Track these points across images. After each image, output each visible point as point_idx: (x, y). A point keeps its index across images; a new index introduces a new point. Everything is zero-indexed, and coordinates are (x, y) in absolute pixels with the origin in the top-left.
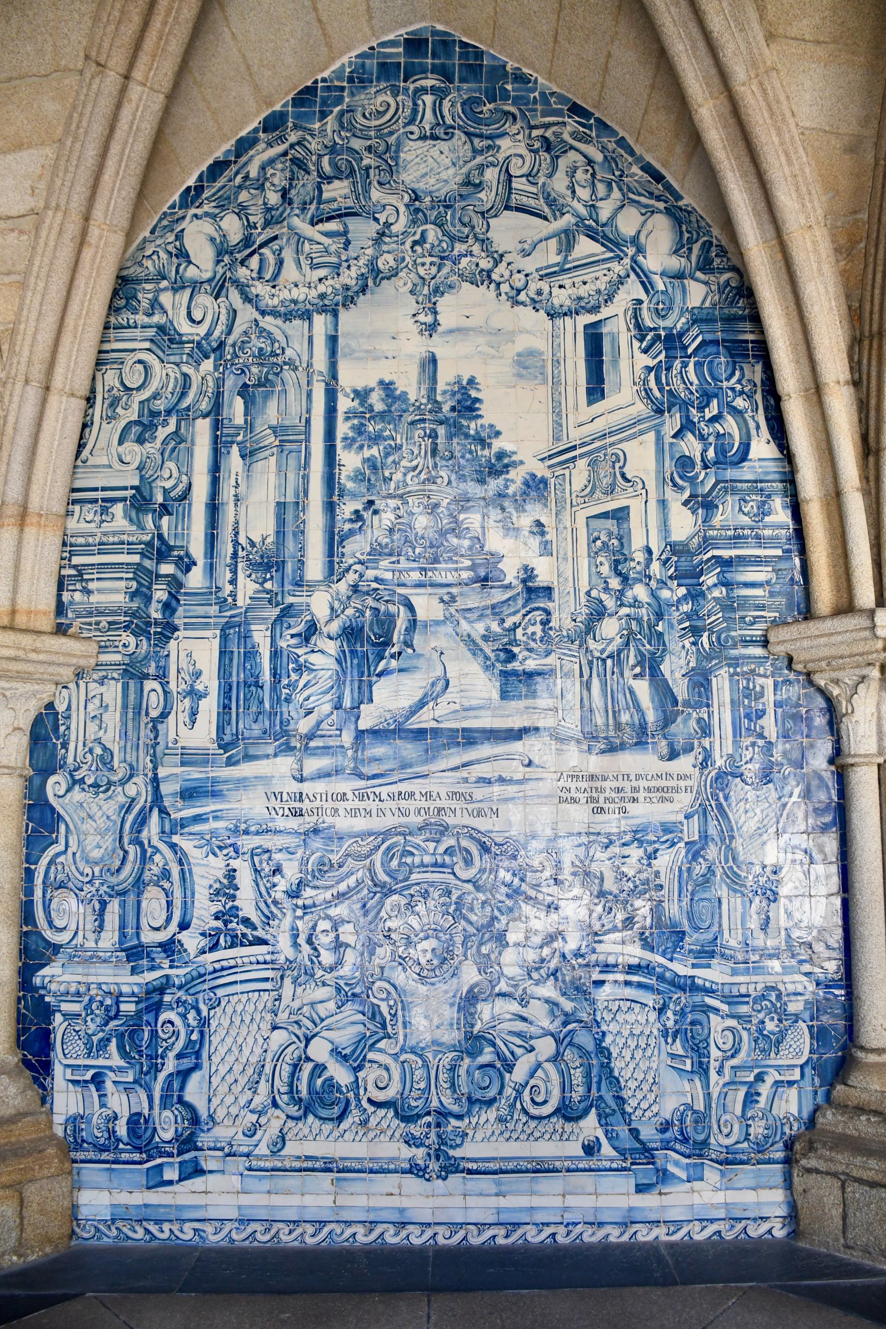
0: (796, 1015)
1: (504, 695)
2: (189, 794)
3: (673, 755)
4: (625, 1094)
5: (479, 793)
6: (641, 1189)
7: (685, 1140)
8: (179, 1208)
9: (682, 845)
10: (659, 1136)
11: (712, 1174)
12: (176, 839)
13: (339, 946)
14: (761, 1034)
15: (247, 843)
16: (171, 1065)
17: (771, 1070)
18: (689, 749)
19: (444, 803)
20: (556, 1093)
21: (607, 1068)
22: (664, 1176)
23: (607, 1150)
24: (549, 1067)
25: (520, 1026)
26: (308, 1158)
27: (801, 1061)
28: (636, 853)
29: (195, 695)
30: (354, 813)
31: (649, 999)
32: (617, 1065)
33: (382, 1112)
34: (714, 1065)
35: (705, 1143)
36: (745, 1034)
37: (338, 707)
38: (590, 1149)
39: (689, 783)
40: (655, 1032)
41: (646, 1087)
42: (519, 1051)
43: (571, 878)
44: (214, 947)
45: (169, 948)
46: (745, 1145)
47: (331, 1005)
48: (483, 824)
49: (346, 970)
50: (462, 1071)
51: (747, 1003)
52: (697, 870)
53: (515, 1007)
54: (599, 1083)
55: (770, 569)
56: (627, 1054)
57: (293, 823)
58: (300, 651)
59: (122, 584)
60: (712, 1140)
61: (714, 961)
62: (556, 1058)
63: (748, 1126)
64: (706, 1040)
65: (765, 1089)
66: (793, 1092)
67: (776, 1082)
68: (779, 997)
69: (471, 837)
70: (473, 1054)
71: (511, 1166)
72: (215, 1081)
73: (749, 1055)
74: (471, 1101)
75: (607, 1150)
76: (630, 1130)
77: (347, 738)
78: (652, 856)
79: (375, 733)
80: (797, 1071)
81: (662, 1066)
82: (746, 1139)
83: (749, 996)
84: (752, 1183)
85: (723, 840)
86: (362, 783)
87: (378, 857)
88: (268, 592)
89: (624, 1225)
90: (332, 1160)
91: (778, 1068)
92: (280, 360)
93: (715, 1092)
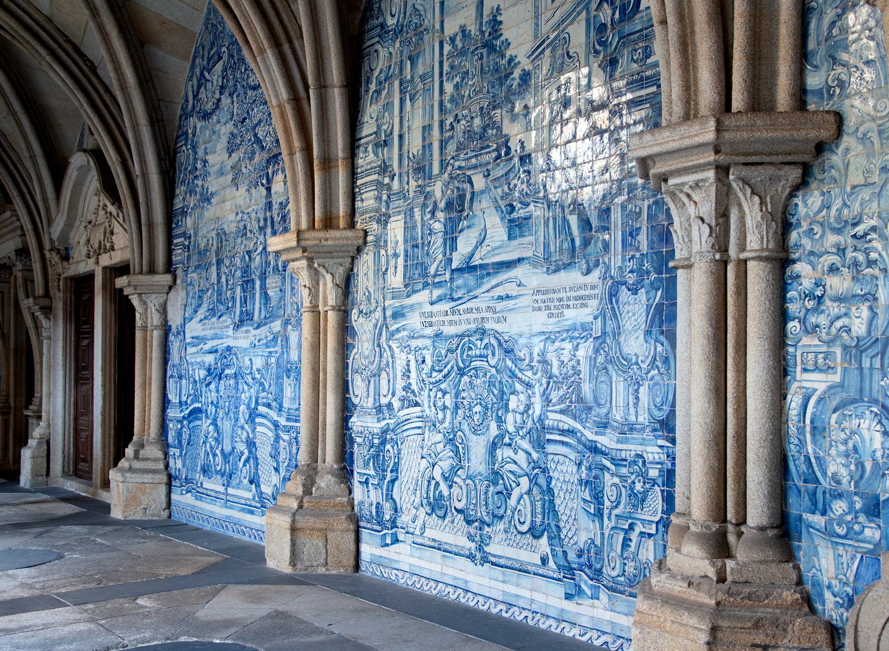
0: (654, 480)
2: (397, 315)
3: (588, 271)
4: (562, 524)
5: (499, 306)
6: (568, 597)
7: (590, 567)
8: (392, 560)
9: (591, 340)
10: (577, 560)
11: (604, 596)
12: (391, 343)
13: (445, 408)
14: (633, 492)
15: (414, 343)
17: (638, 522)
18: (597, 265)
19: (484, 315)
21: (552, 502)
22: (580, 592)
23: (551, 564)
24: (525, 496)
26: (434, 540)
27: (657, 519)
28: (568, 346)
29: (396, 255)
30: (451, 323)
31: (573, 455)
32: (557, 502)
33: (459, 516)
34: (606, 512)
35: (600, 571)
36: (623, 490)
37: (445, 255)
38: (544, 561)
39: (596, 291)
40: (576, 481)
41: (571, 521)
42: (514, 485)
43: (537, 364)
46: (622, 579)
47: (441, 445)
48: (499, 327)
49: (447, 424)
50: (490, 494)
51: (625, 466)
52: (599, 361)
54: (548, 513)
55: (648, 105)
56: (562, 494)
57: (429, 331)
58: (431, 222)
59: (372, 193)
60: (604, 571)
61: (608, 431)
62: (529, 492)
63: (625, 564)
64: (602, 491)
65: (634, 536)
66: (650, 543)
67: (641, 533)
68: (644, 462)
69: (495, 337)
70: (495, 484)
71: (509, 563)
72: (403, 486)
73: (625, 508)
74: (494, 516)
75: (551, 564)
76: (563, 551)
77: (448, 276)
78: (576, 348)
79: (459, 270)
80: (654, 526)
81: (579, 507)
82: (623, 575)
83: (626, 460)
84: (625, 610)
85: (614, 335)
86: (454, 304)
87: (459, 351)
88: (419, 186)
89: (559, 620)
90: (440, 543)
91: (643, 521)
92: (421, 29)
93: (607, 532)
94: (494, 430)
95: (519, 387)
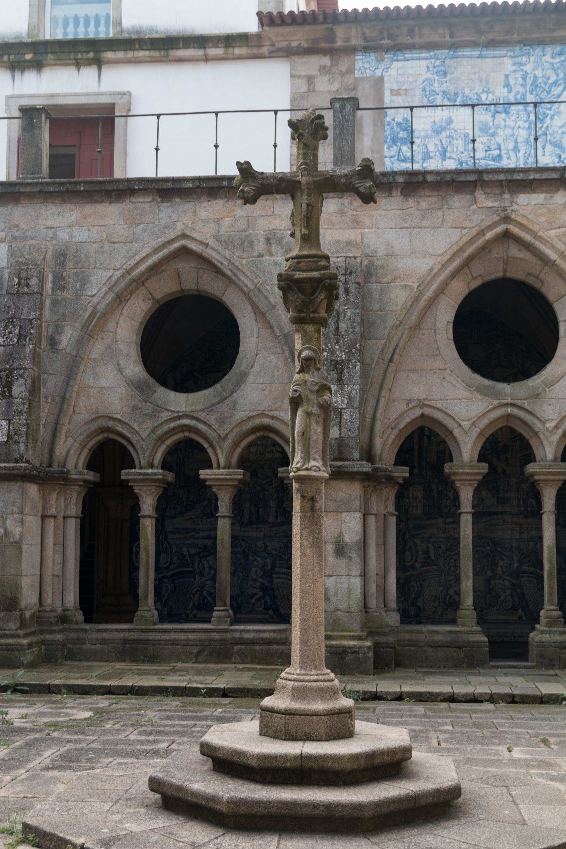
1: (497, 503)
16: (413, 596)
20: (511, 603)
24: (510, 597)
25: (502, 586)
44: (424, 566)
45: (413, 567)
53: (500, 582)
62: (511, 595)
94: (489, 573)
95: (504, 558)
